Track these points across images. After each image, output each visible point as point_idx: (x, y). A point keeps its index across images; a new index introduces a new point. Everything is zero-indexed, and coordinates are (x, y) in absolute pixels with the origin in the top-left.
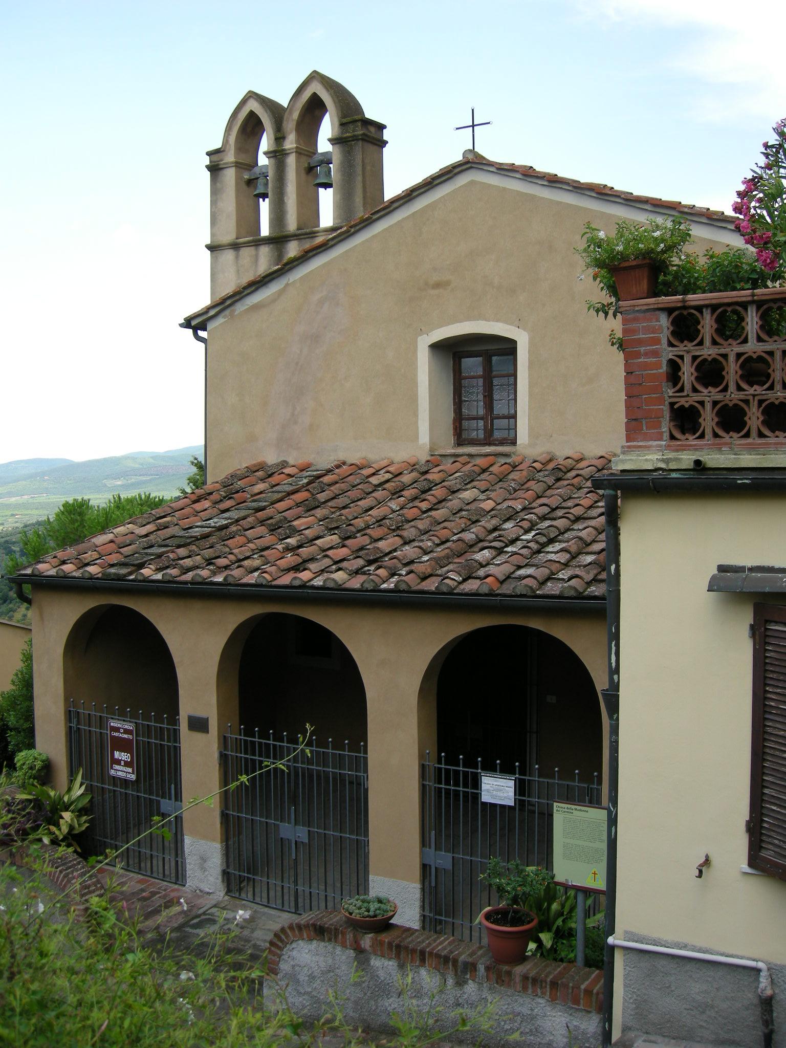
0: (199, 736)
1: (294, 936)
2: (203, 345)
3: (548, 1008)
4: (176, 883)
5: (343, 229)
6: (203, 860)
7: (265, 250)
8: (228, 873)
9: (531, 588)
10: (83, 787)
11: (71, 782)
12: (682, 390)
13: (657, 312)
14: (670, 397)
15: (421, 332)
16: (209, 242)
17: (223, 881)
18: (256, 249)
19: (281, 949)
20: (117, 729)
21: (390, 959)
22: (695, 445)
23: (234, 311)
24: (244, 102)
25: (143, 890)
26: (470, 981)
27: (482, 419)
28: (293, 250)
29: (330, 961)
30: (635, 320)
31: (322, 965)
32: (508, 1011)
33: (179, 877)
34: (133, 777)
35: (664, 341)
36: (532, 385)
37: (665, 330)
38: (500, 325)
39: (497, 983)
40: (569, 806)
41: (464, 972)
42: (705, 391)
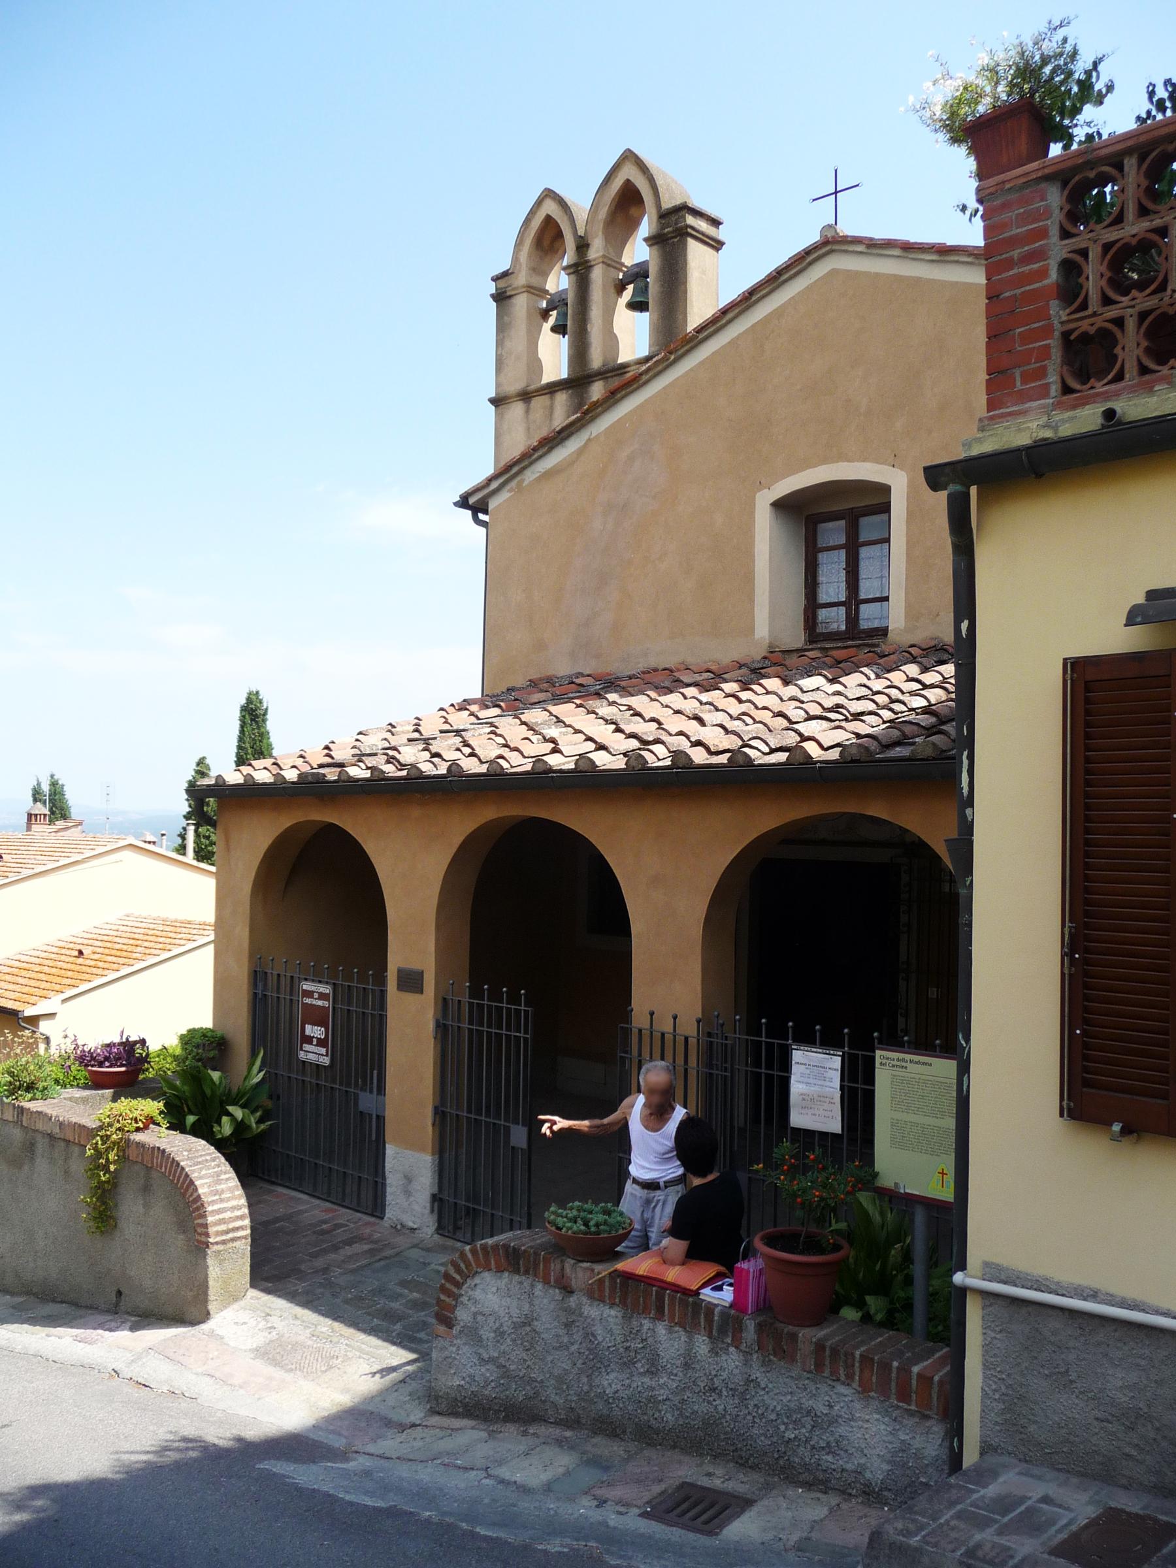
0: (410, 998)
1: (478, 1266)
2: (484, 530)
3: (857, 1405)
4: (373, 1215)
5: (660, 357)
6: (408, 1179)
7: (562, 398)
8: (441, 1199)
9: (867, 749)
10: (262, 1074)
11: (251, 1065)
12: (1084, 306)
13: (1043, 185)
14: (1062, 323)
15: (761, 486)
16: (493, 395)
17: (432, 1211)
18: (552, 399)
19: (459, 1285)
20: (309, 994)
21: (612, 1305)
22: (1106, 392)
23: (523, 480)
24: (539, 203)
25: (325, 1222)
26: (732, 1349)
27: (853, 619)
28: (597, 391)
29: (526, 1308)
30: (1005, 206)
31: (515, 1312)
32: (792, 1405)
33: (377, 1207)
34: (326, 1061)
35: (1054, 232)
36: (911, 545)
37: (1057, 211)
38: (868, 465)
39: (775, 1355)
40: (901, 1056)
41: (722, 1331)
42: (1125, 300)
